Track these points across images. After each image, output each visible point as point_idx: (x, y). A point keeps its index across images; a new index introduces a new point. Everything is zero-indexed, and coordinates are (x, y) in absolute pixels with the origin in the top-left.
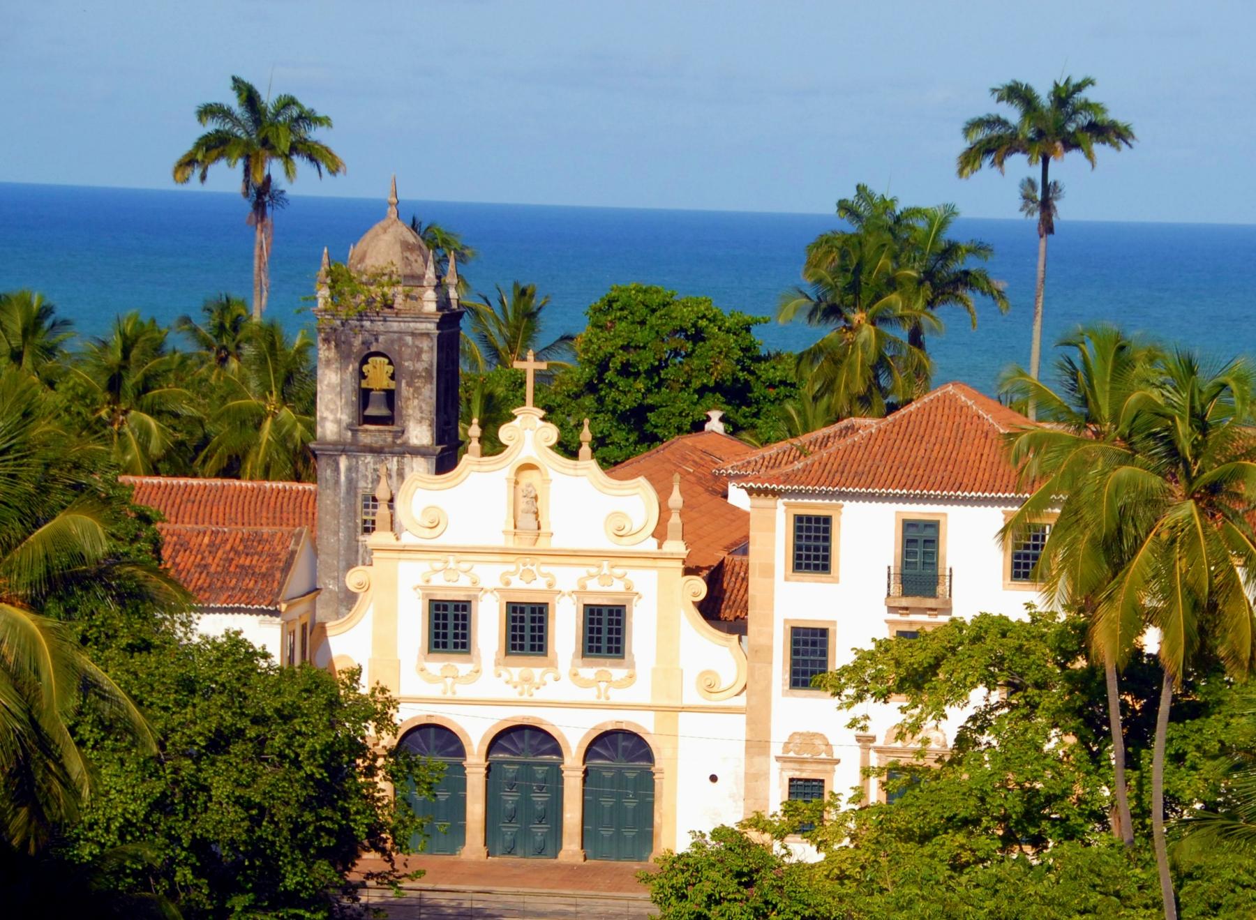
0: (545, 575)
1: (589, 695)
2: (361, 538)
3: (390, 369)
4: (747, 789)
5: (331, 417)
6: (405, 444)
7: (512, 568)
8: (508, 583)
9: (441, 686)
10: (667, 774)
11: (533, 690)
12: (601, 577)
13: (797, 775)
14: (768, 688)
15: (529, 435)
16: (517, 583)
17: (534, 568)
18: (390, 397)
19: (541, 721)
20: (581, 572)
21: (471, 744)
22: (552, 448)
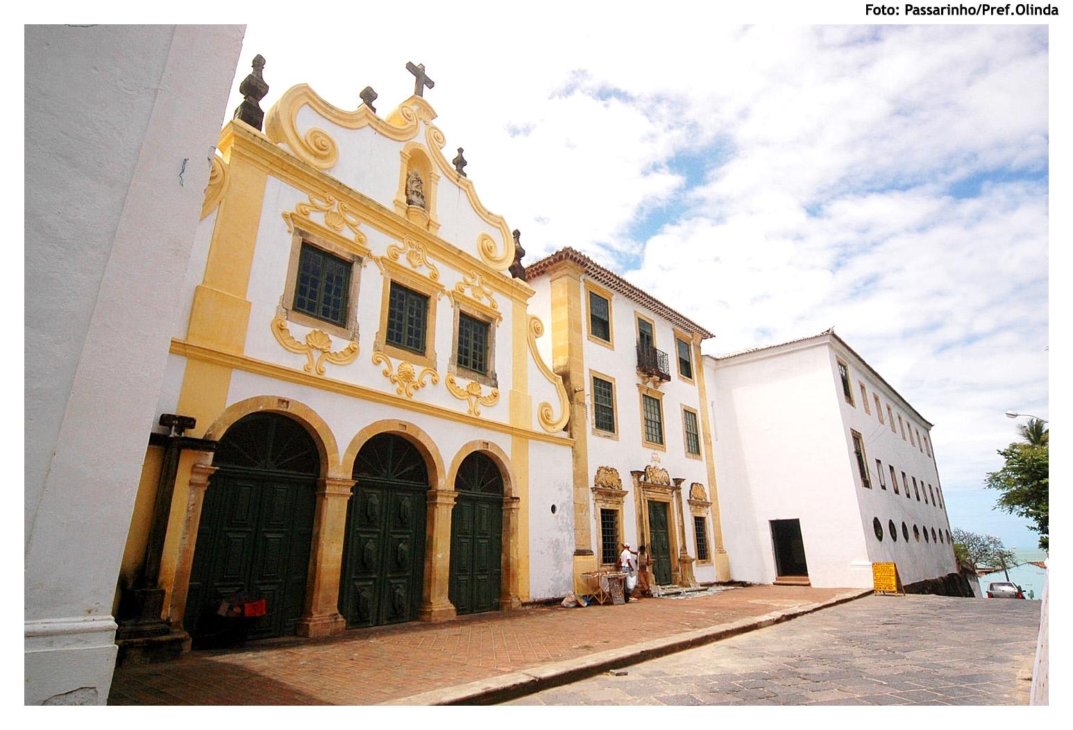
0: (428, 265)
1: (462, 408)
10: (521, 504)
11: (412, 391)
12: (474, 288)
19: (419, 430)
21: (336, 451)
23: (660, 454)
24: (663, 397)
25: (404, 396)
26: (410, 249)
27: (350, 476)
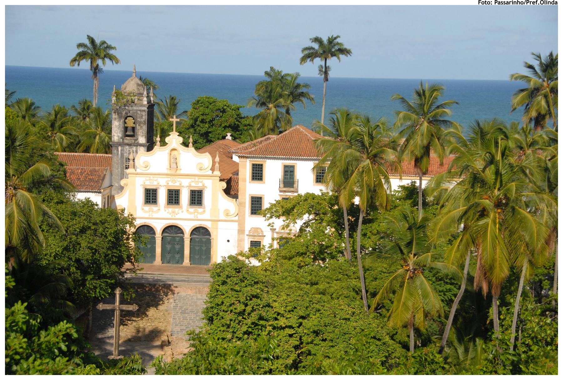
0: (179, 181)
1: (192, 217)
2: (125, 170)
3: (133, 121)
4: (238, 244)
5: (116, 135)
6: (138, 143)
7: (169, 179)
8: (168, 184)
9: (148, 214)
12: (195, 182)
13: (253, 240)
14: (244, 215)
15: (174, 140)
16: (171, 184)
17: (176, 179)
18: (133, 129)
20: (190, 180)
21: (157, 231)
22: (181, 144)
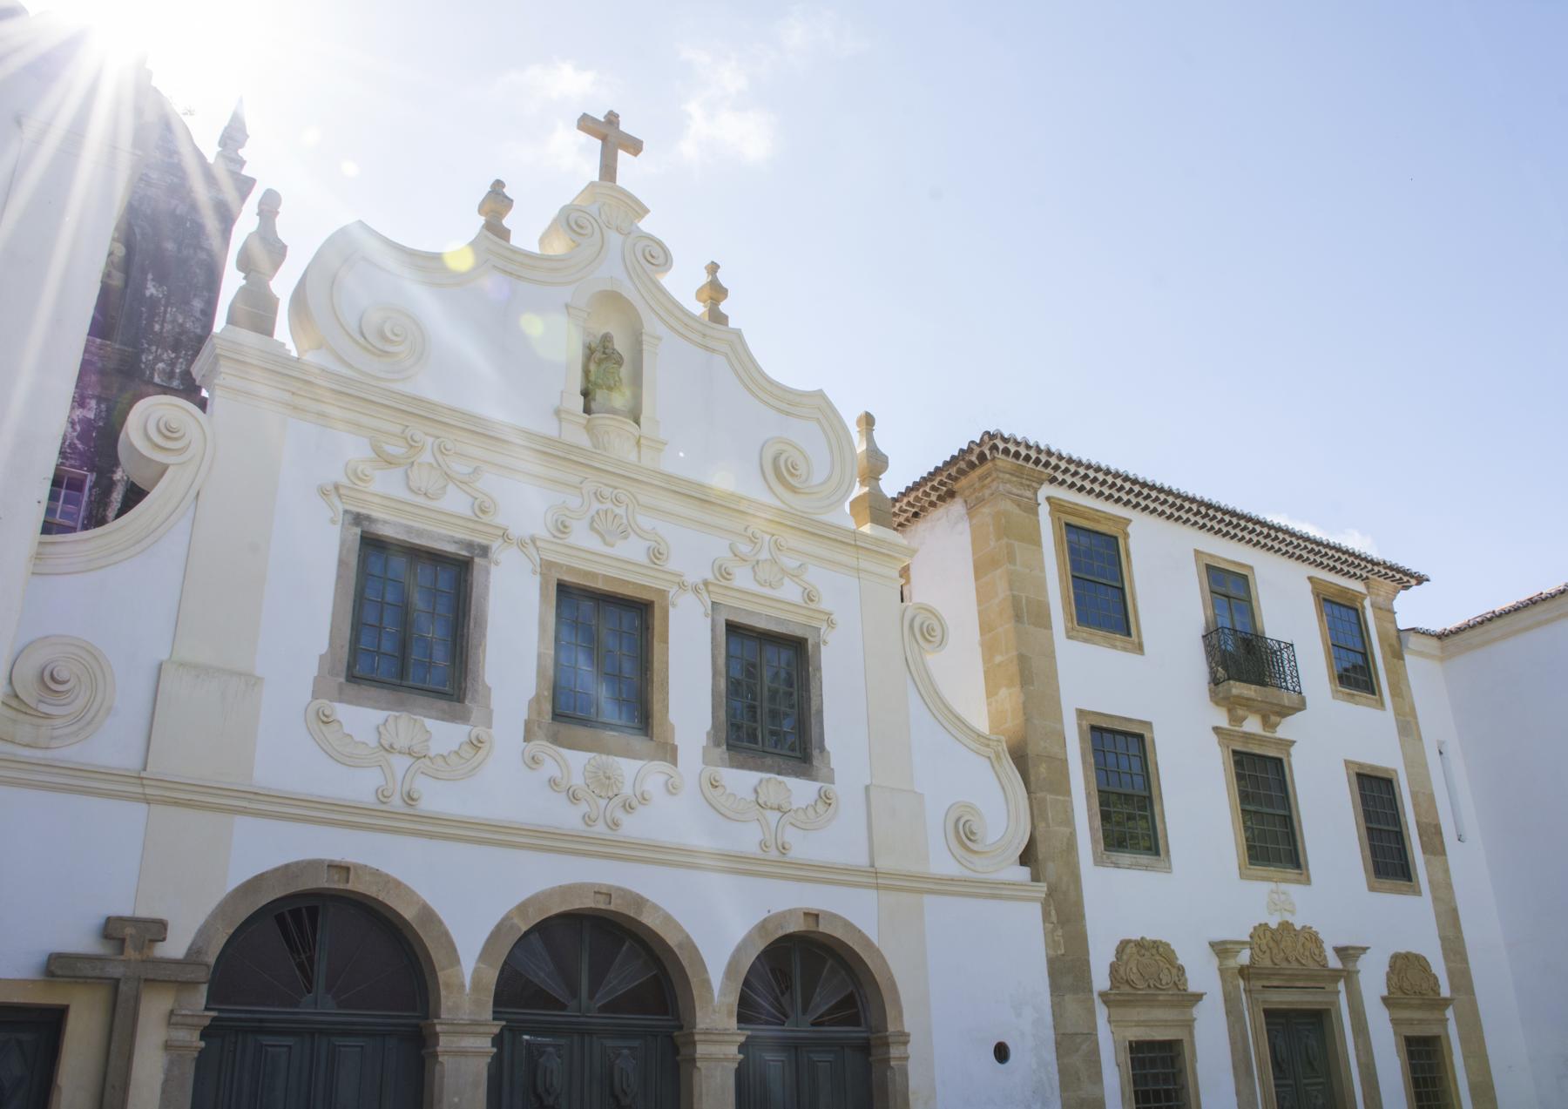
11: (620, 815)
16: (582, 537)
19: (640, 902)
21: (455, 960)
23: (1294, 891)
24: (1293, 750)
25: (600, 829)
26: (596, 506)
27: (488, 1014)
